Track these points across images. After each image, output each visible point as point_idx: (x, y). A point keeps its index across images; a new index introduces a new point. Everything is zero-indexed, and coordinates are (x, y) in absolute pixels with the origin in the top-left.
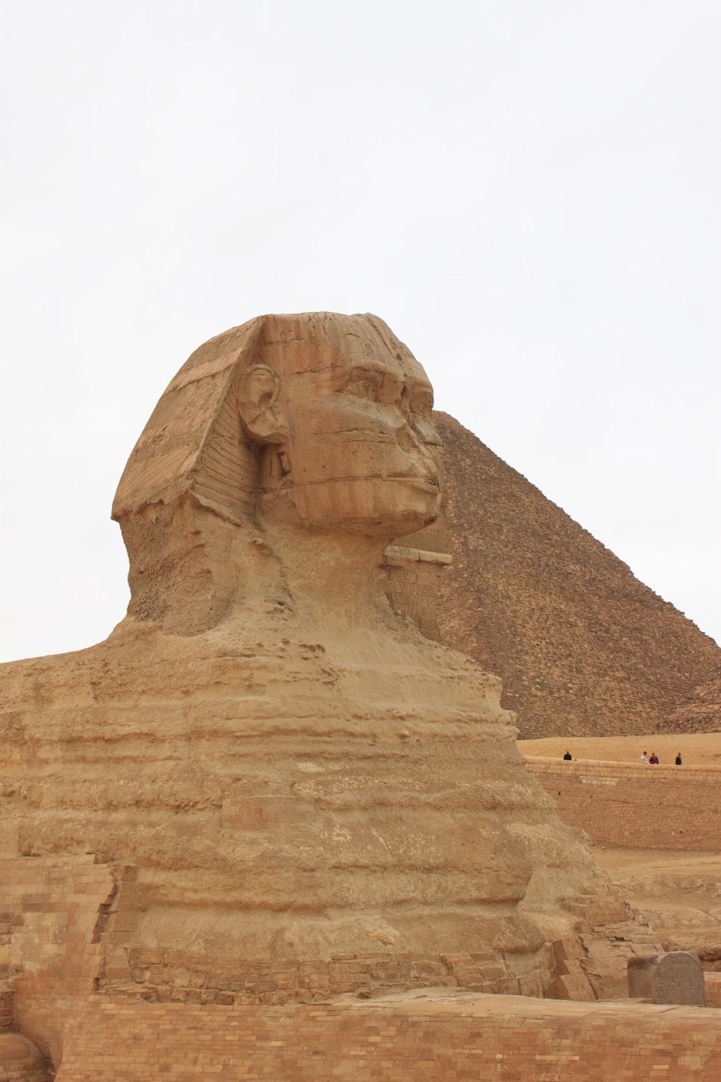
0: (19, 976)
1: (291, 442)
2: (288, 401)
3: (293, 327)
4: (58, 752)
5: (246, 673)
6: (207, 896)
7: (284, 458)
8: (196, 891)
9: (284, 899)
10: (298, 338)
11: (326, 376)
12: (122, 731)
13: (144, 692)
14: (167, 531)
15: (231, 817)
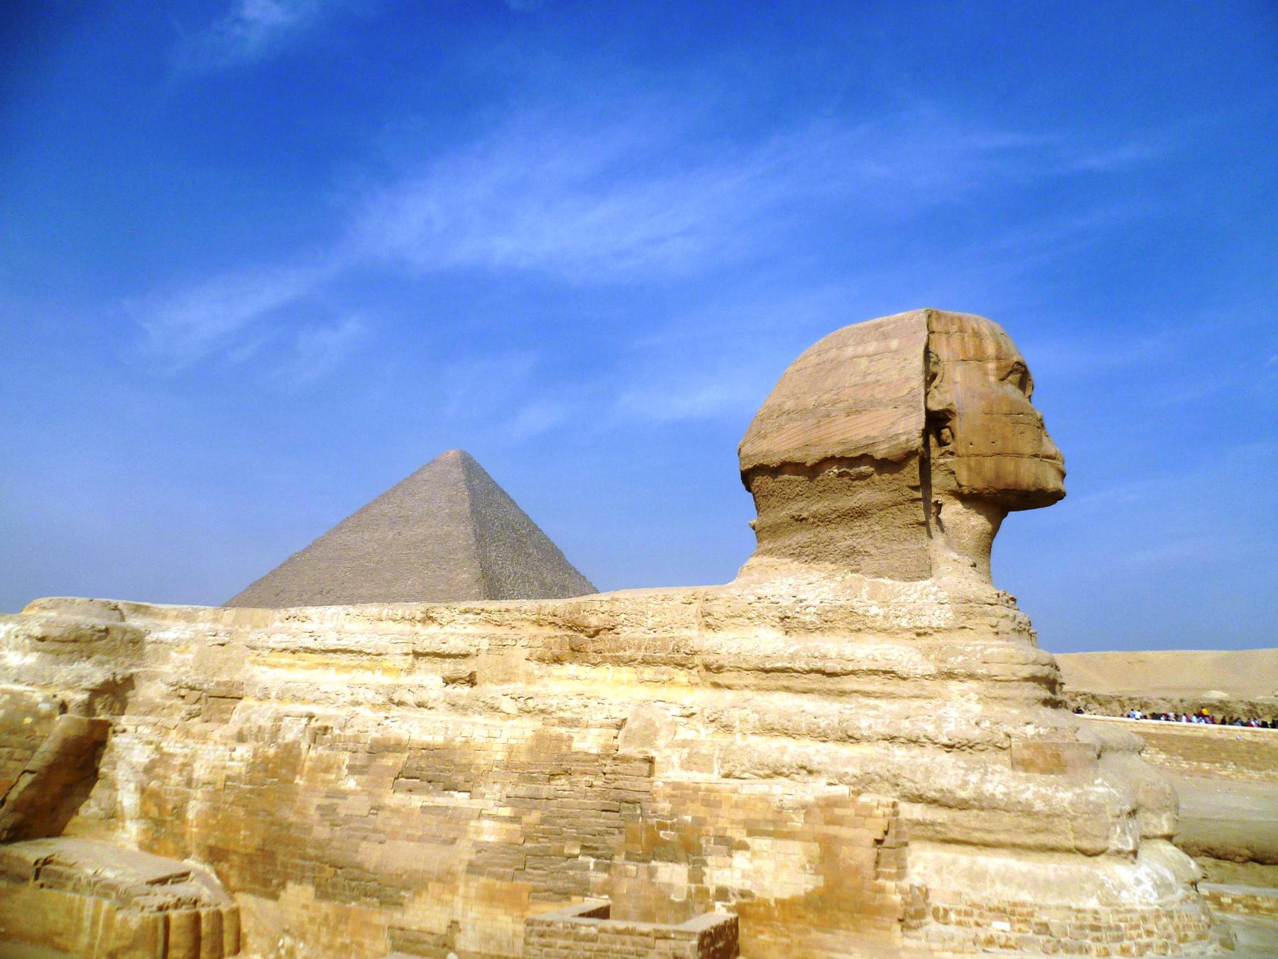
0: (745, 901)
1: (957, 419)
2: (955, 383)
3: (957, 321)
4: (750, 679)
5: (994, 621)
6: (1003, 837)
7: (946, 432)
8: (989, 832)
9: (1100, 845)
10: (961, 330)
11: (991, 366)
12: (850, 667)
13: (860, 630)
14: (854, 483)
15: (1023, 760)
